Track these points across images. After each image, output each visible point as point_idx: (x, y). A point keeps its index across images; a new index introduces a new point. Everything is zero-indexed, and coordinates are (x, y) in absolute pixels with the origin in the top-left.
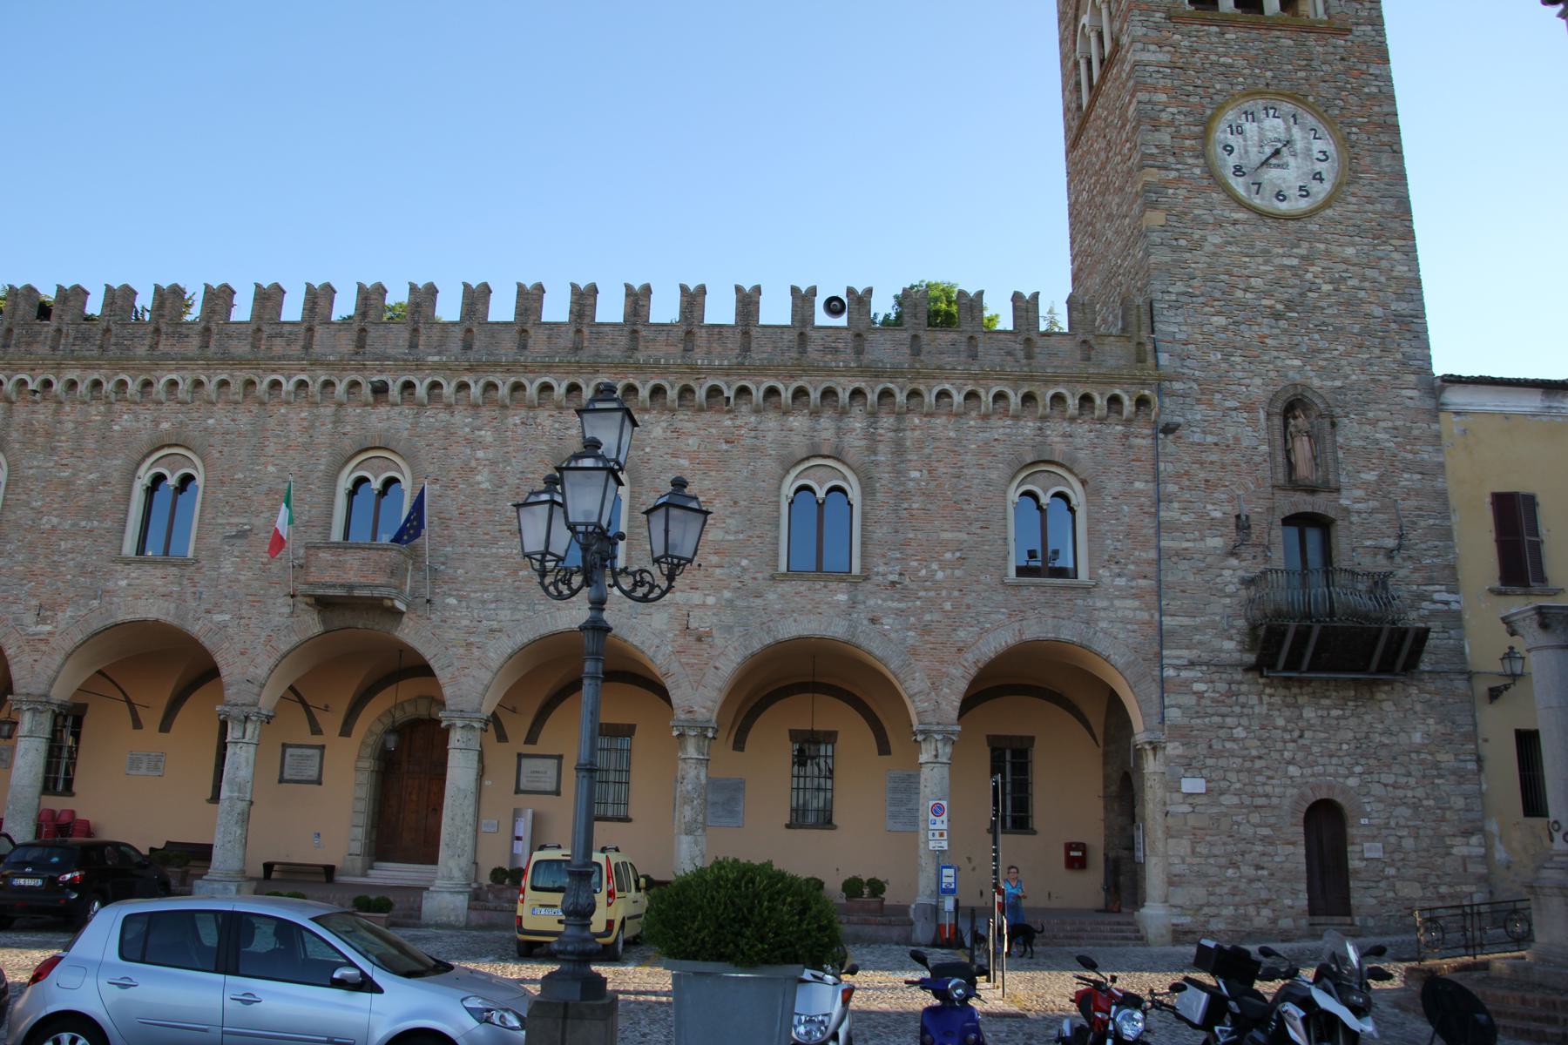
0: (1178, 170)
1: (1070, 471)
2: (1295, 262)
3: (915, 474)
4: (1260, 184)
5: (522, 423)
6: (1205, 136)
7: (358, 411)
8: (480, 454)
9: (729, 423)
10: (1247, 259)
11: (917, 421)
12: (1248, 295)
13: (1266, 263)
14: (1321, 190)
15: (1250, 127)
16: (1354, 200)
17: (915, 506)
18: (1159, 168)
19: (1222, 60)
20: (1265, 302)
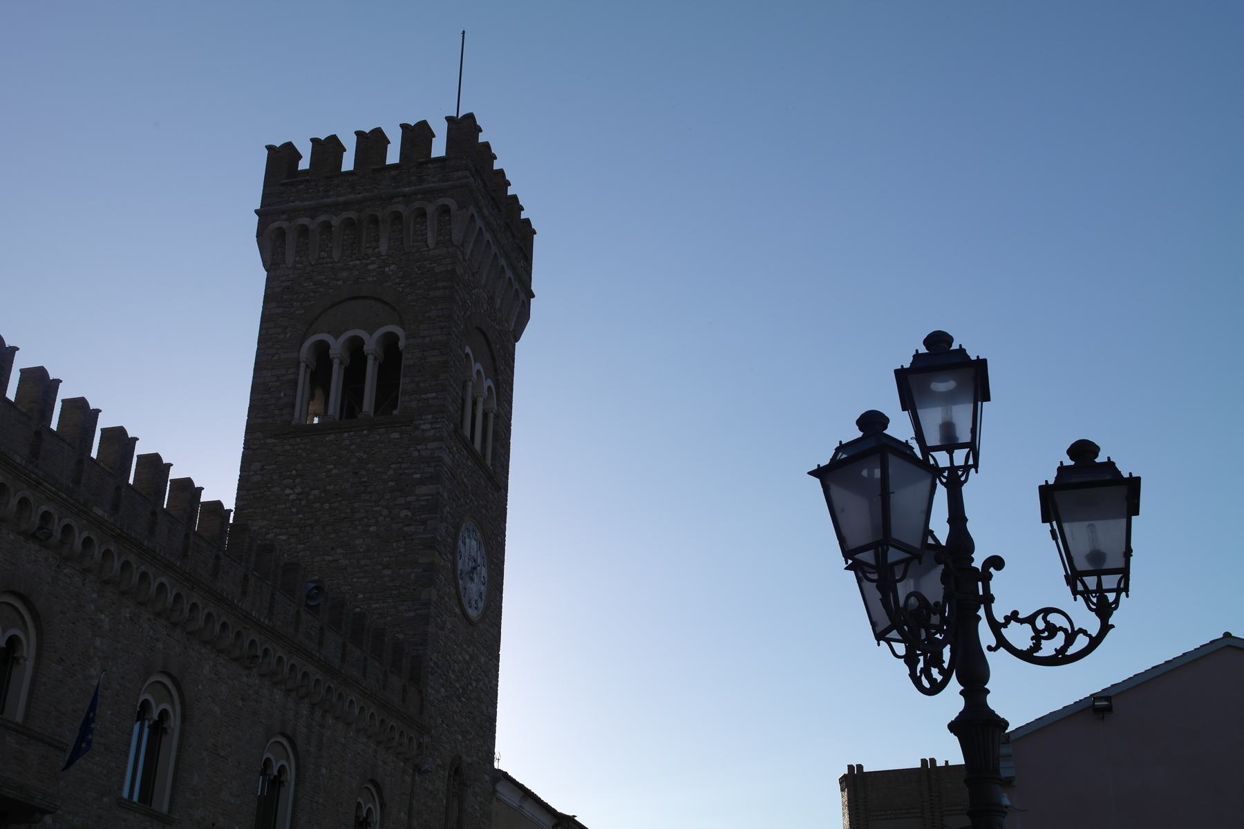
0: (444, 560)
1: (379, 791)
2: (467, 658)
3: (324, 771)
4: (465, 589)
5: (131, 619)
6: (455, 538)
7: (11, 537)
8: (98, 642)
9: (245, 679)
10: (456, 647)
11: (330, 721)
12: (453, 677)
13: (461, 654)
14: (481, 605)
15: (467, 541)
16: (487, 620)
17: (321, 801)
18: (440, 554)
19: (465, 480)
20: (458, 685)
